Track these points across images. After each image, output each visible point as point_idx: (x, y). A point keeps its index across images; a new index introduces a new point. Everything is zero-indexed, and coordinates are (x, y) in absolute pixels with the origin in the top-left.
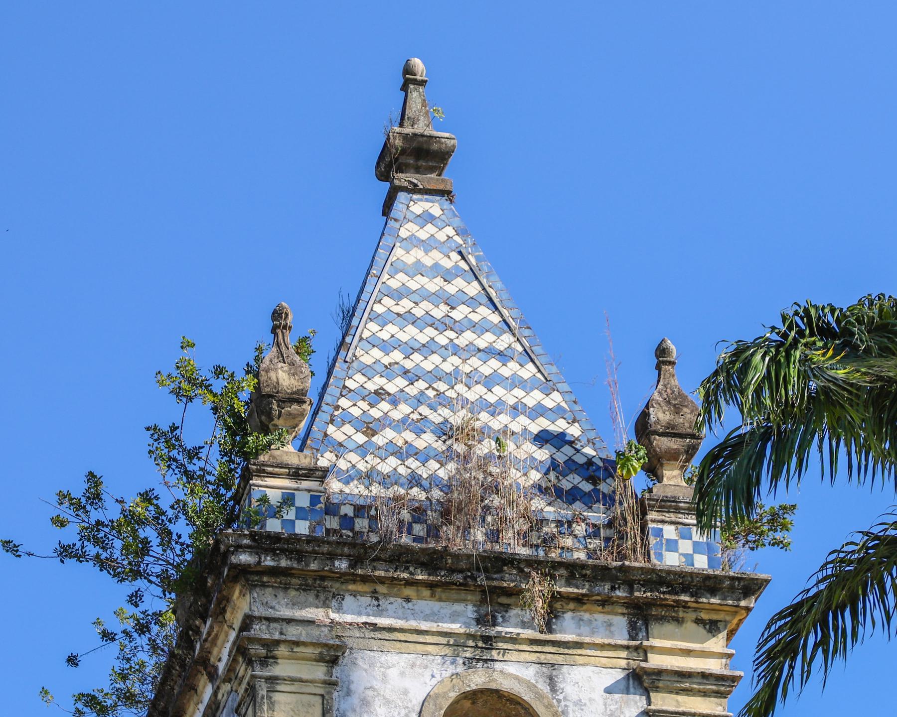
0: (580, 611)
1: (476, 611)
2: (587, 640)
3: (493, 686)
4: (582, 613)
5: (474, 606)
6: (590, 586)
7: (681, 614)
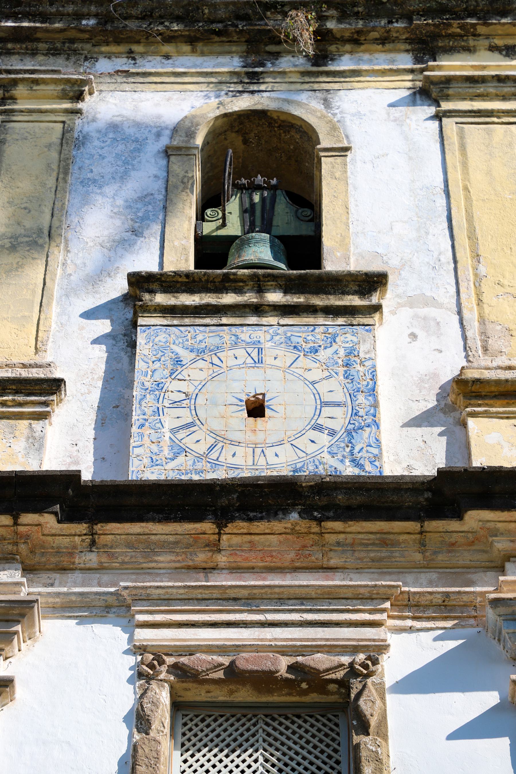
0: (357, 52)
1: (243, 61)
2: (365, 67)
3: (259, 107)
4: (361, 54)
5: (241, 57)
6: (365, 22)
7: (471, 43)
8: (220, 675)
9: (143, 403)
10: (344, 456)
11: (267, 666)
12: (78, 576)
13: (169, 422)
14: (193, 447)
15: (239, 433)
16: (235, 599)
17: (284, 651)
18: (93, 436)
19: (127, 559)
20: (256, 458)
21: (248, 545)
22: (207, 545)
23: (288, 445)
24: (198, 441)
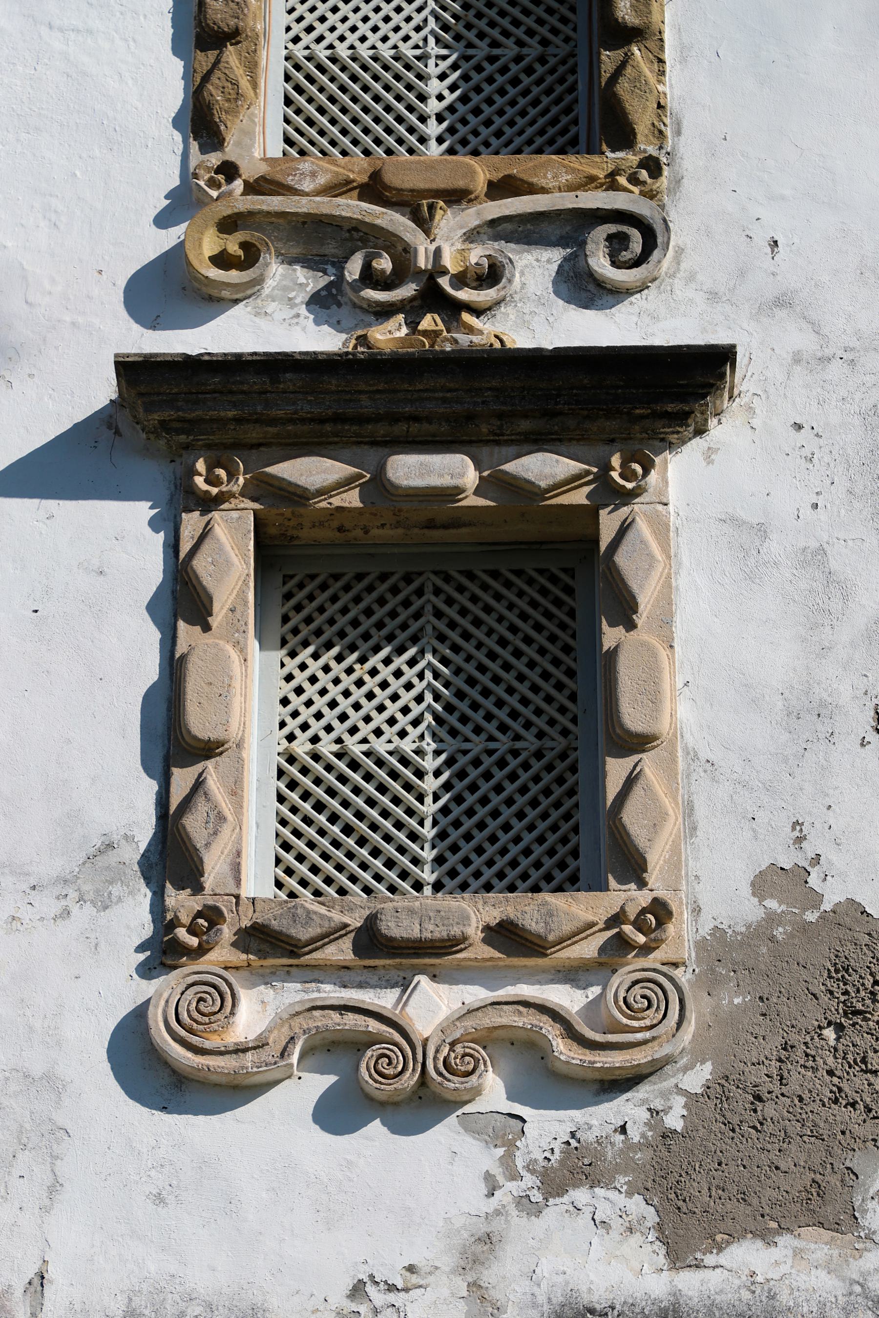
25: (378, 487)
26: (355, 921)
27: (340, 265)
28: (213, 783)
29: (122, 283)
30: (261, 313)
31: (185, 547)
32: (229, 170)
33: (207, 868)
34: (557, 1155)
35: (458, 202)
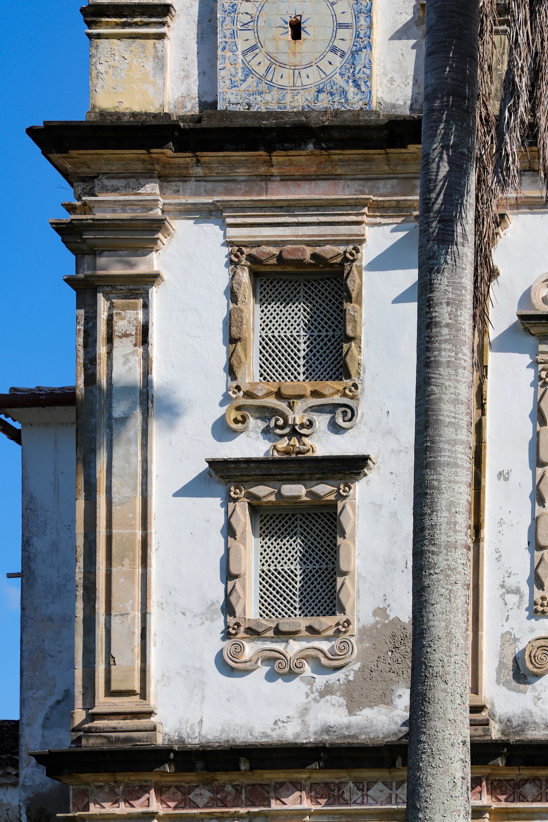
8: (274, 261)
9: (224, 26)
10: (349, 77)
11: (298, 256)
12: (192, 184)
13: (242, 46)
14: (256, 68)
15: (284, 55)
16: (281, 207)
17: (309, 244)
18: (196, 51)
19: (220, 171)
20: (296, 79)
21: (288, 162)
22: (265, 162)
23: (315, 67)
24: (259, 63)
25: (279, 494)
26: (274, 625)
27: (270, 420)
28: (238, 587)
29: (211, 426)
30: (248, 436)
31: (229, 514)
32: (238, 388)
33: (236, 611)
34: (323, 688)
35: (302, 398)
